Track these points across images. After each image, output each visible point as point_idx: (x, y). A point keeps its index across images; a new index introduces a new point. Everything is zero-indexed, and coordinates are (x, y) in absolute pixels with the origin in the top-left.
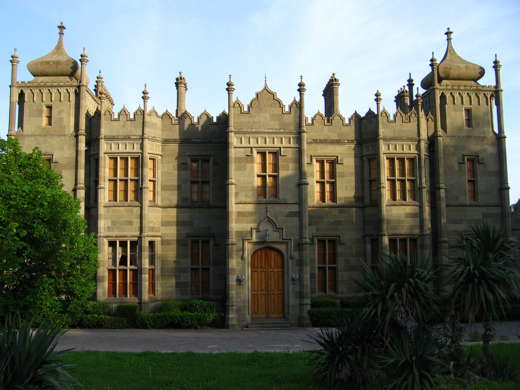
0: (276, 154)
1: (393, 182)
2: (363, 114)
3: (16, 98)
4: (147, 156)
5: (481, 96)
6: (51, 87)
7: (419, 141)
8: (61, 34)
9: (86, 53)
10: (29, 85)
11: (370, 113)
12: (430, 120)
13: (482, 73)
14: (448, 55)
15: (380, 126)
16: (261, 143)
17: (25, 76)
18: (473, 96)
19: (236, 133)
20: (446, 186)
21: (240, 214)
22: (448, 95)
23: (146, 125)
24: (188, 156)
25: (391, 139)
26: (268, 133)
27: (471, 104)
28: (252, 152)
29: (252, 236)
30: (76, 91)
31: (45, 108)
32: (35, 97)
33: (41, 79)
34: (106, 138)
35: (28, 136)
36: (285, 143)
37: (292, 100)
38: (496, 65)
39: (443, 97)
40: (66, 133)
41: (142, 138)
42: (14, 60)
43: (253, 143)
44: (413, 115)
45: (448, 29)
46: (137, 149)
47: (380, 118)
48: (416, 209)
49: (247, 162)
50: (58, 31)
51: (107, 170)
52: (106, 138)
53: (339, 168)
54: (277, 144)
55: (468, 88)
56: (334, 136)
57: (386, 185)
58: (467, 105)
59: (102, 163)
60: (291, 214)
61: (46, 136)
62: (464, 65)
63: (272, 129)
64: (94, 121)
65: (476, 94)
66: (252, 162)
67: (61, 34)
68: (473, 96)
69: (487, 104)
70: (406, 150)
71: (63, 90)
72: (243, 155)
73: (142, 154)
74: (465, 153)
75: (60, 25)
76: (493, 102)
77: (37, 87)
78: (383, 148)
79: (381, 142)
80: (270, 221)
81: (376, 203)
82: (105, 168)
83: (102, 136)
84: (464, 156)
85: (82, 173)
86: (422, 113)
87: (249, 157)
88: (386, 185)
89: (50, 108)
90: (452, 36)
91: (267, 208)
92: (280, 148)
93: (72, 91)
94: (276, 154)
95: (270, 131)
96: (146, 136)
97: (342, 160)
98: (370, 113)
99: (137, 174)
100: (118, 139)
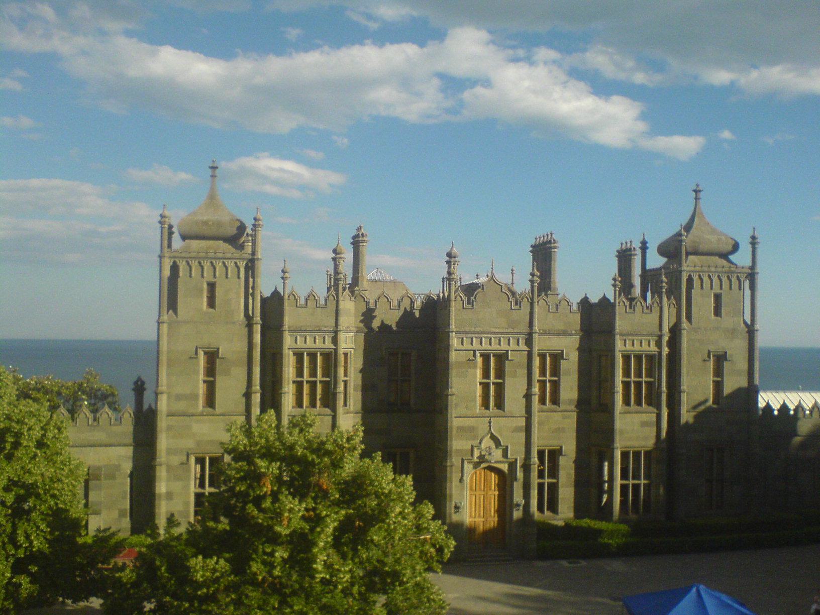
0: (502, 358)
1: (626, 385)
2: (594, 299)
3: (167, 273)
4: (341, 352)
5: (734, 280)
7: (660, 337)
9: (259, 216)
10: (183, 255)
11: (604, 299)
12: (672, 306)
13: (736, 247)
14: (696, 219)
15: (617, 318)
16: (485, 346)
18: (725, 279)
19: (457, 333)
20: (688, 387)
21: (461, 429)
22: (695, 278)
23: (341, 312)
25: (628, 335)
26: (494, 333)
27: (721, 288)
28: (474, 355)
29: (472, 455)
30: (246, 265)
31: (205, 286)
32: (193, 271)
33: (195, 244)
34: (294, 331)
35: (186, 322)
36: (513, 346)
38: (754, 242)
39: (690, 280)
41: (336, 332)
43: (476, 345)
44: (656, 305)
45: (698, 185)
46: (329, 344)
47: (617, 307)
48: (653, 417)
49: (470, 367)
50: (210, 171)
51: (291, 369)
52: (294, 331)
53: (563, 364)
54: (504, 346)
55: (719, 269)
56: (561, 327)
57: (619, 388)
58: (716, 289)
59: (285, 361)
60: (517, 429)
62: (716, 237)
64: (273, 307)
65: (728, 277)
66: (475, 367)
68: (725, 279)
69: (740, 289)
70: (645, 346)
71: (231, 265)
72: (464, 360)
73: (336, 350)
74: (712, 348)
76: (747, 284)
77: (195, 258)
78: (619, 345)
79: (618, 337)
80: (493, 437)
81: (607, 409)
82: (289, 367)
83: (286, 327)
84: (709, 352)
85: (257, 370)
86: (665, 299)
87: (471, 362)
88: (619, 388)
89: (212, 286)
90: (701, 195)
91: (490, 422)
92: (507, 351)
93: (242, 265)
94: (502, 358)
96: (340, 328)
97: (567, 354)
98: (604, 299)
99: (326, 373)
100: (306, 331)
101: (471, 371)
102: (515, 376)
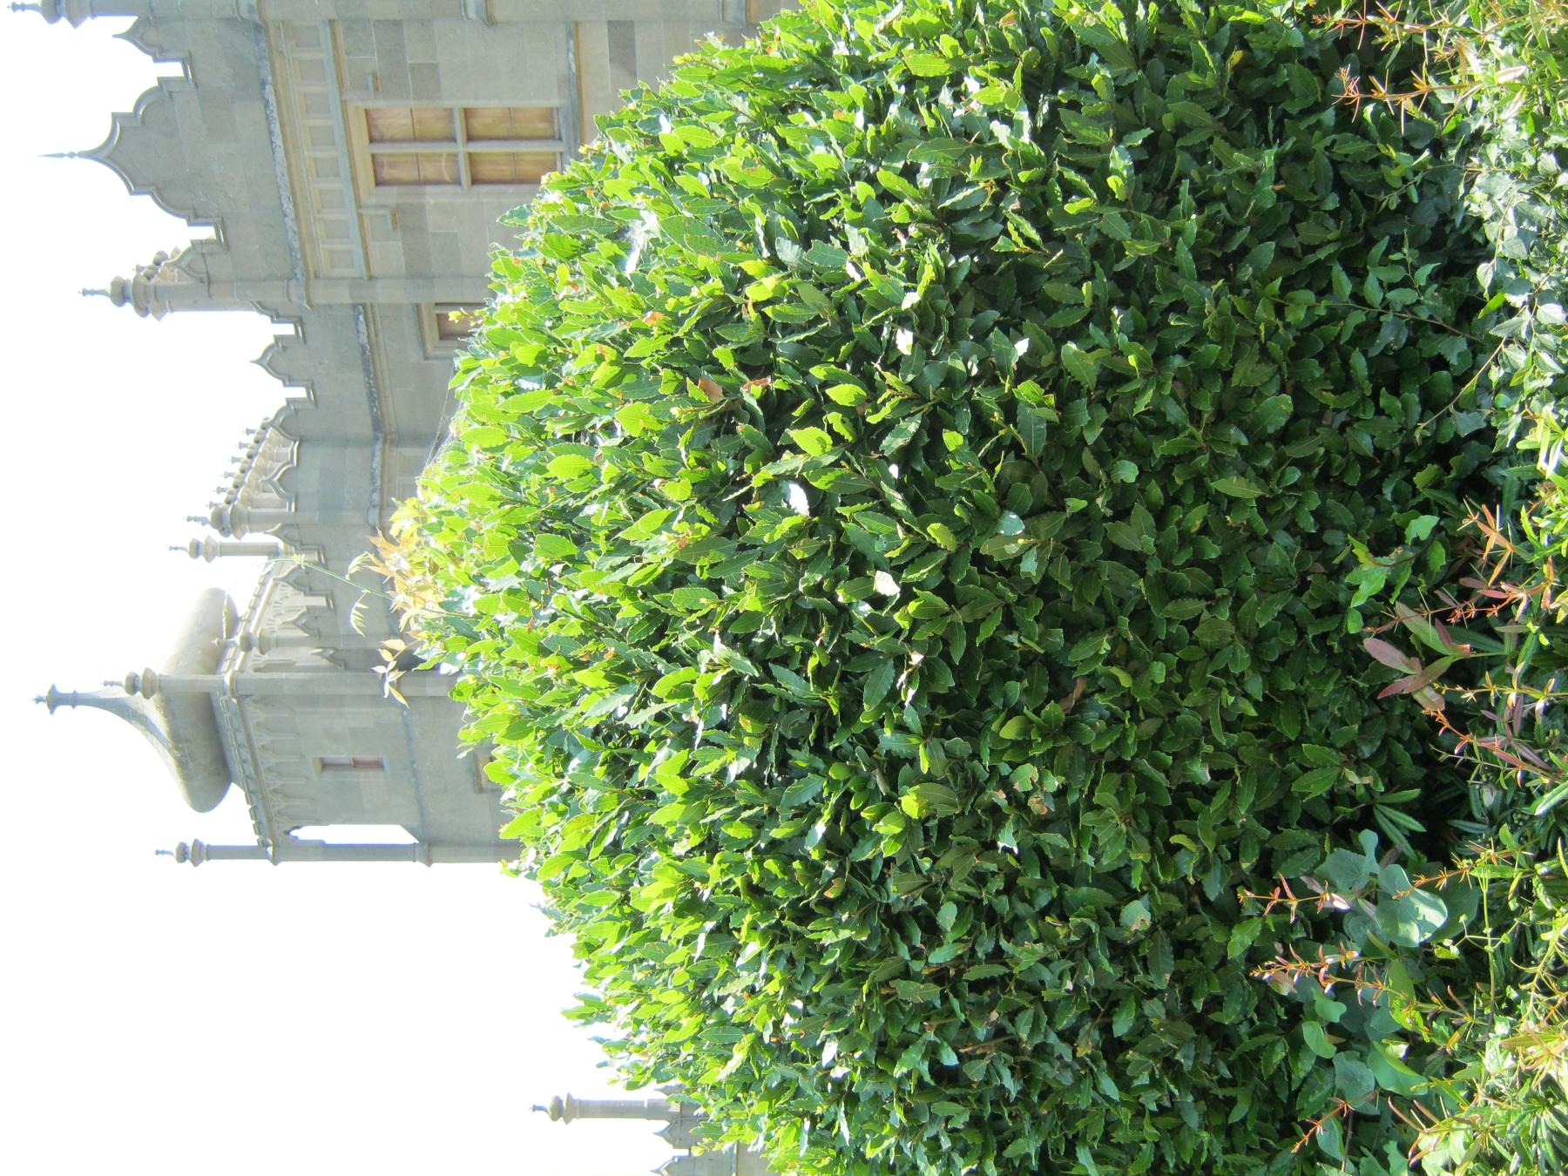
6: (256, 766)
8: (74, 700)
17: (233, 817)
24: (426, 358)
31: (329, 776)
37: (129, 48)
40: (400, 720)
42: (194, 853)
50: (62, 710)
61: (415, 773)
63: (271, 133)
67: (74, 700)
75: (44, 706)
89: (325, 765)
95: (279, 141)
101: (432, 221)
102: (434, 68)
